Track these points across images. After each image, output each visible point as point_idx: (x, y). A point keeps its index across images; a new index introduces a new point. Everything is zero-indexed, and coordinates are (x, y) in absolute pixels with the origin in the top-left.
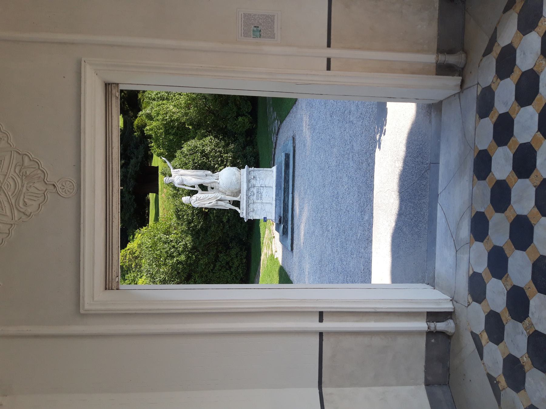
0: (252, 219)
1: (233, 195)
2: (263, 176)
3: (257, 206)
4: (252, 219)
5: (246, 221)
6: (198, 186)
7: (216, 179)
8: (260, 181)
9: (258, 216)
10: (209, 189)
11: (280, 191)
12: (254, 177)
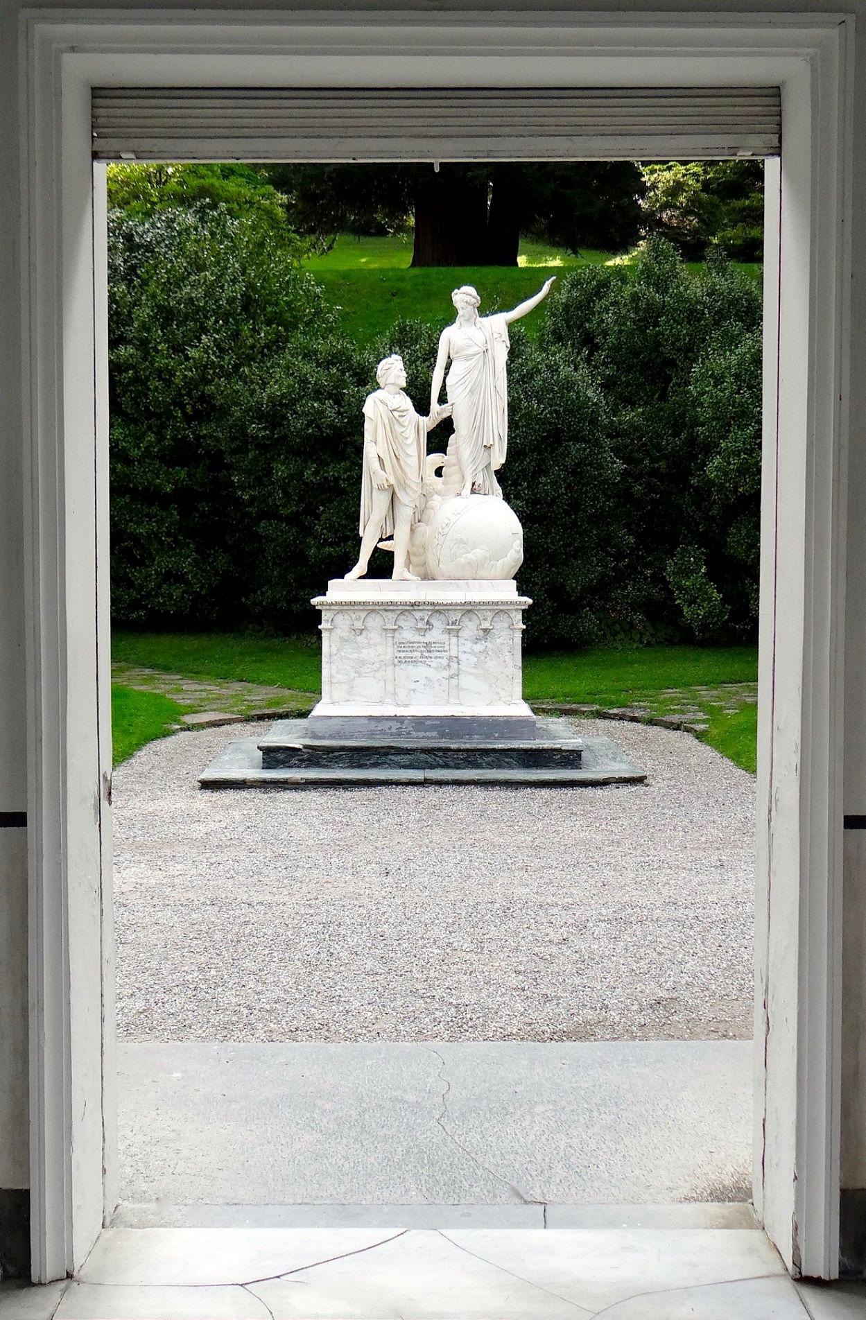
0: (319, 627)
3: (376, 646)
4: (319, 627)
5: (314, 601)
6: (445, 415)
7: (474, 484)
8: (473, 653)
9: (334, 650)
10: (436, 459)
12: (485, 630)
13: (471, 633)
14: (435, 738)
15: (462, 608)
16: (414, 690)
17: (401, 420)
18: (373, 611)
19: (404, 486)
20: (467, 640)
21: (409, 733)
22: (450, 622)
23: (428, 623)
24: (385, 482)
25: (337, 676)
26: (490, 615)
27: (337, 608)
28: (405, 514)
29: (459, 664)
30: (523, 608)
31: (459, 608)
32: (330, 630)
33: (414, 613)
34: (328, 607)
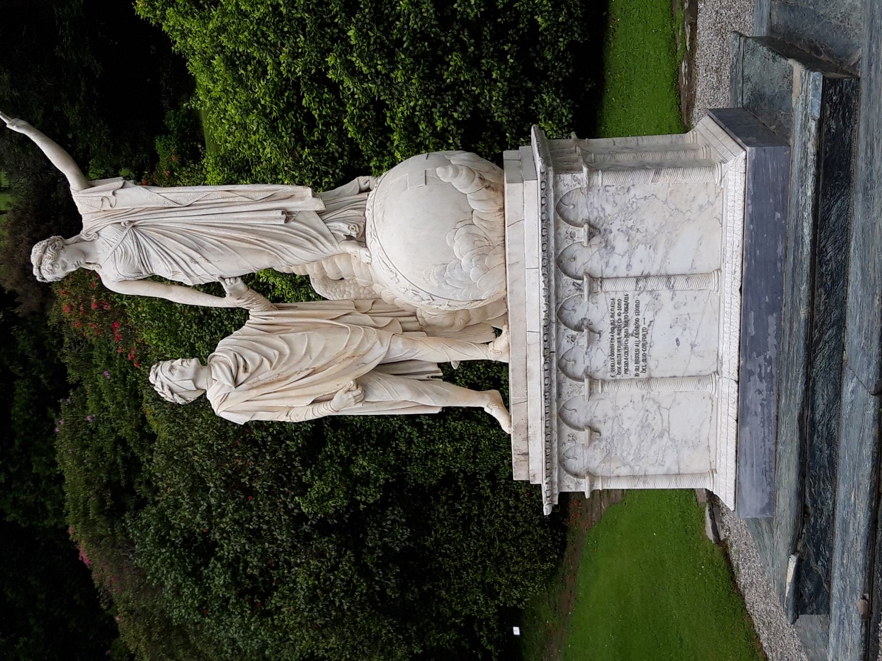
2: (650, 222)
8: (630, 252)
12: (593, 231)
13: (597, 256)
14: (779, 320)
15: (553, 278)
16: (693, 346)
17: (251, 368)
18: (560, 414)
19: (357, 357)
20: (607, 263)
21: (769, 362)
22: (578, 293)
23: (578, 328)
24: (350, 395)
25: (667, 464)
26: (565, 228)
27: (556, 474)
28: (400, 349)
31: (553, 283)
33: (562, 353)
34: (556, 486)
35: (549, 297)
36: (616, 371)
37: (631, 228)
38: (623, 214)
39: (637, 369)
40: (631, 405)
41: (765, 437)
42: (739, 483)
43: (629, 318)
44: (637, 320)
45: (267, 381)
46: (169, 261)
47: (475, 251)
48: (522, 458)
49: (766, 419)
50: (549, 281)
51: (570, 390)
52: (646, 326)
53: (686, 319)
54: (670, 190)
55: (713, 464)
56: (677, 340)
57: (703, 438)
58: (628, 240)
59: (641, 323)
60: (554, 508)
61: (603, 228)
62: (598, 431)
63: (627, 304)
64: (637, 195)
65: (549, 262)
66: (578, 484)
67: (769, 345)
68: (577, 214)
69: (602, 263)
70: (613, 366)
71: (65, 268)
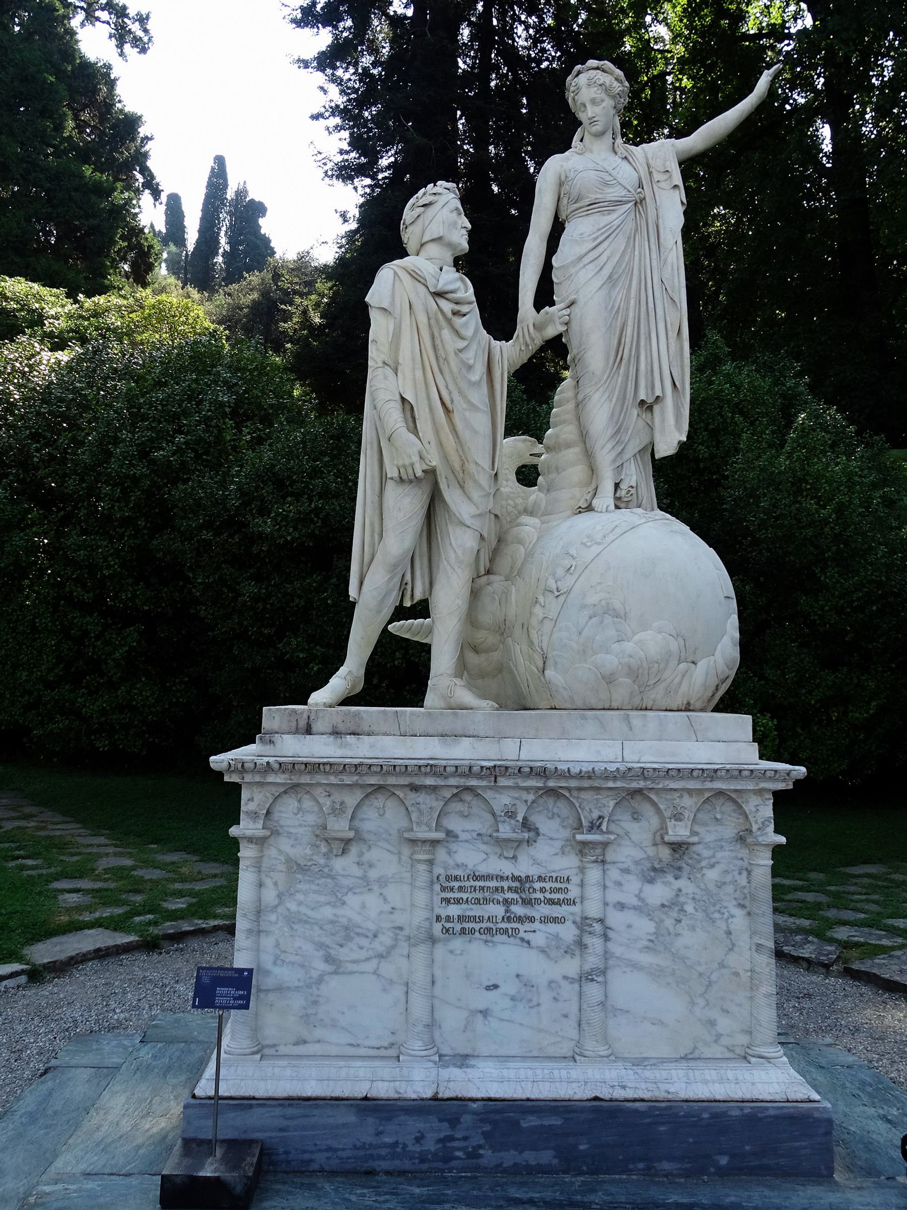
1: (481, 636)
4: (234, 831)
5: (218, 761)
7: (617, 486)
8: (642, 908)
9: (270, 895)
11: (546, 1157)
12: (678, 848)
13: (638, 854)
15: (619, 784)
16: (485, 1013)
18: (380, 788)
20: (626, 871)
21: (473, 1155)
24: (416, 458)
25: (277, 970)
27: (280, 778)
29: (606, 938)
30: (781, 786)
31: (611, 784)
32: (260, 842)
34: (258, 778)
35: (590, 778)
36: (447, 884)
37: (682, 910)
38: (705, 898)
39: (448, 919)
40: (387, 908)
41: (336, 1150)
42: (251, 1107)
43: (537, 907)
44: (531, 920)
45: (438, 342)
46: (597, 237)
47: (645, 664)
48: (302, 723)
49: (369, 1152)
50: (615, 779)
51: (422, 807)
52: (522, 934)
53: (530, 1001)
54: (741, 972)
55: (272, 1051)
56: (496, 987)
57: (319, 1033)
58: (663, 906)
59: (528, 926)
60: (220, 774)
61: (684, 865)
62: (344, 852)
63: (558, 903)
64: (734, 920)
65: (645, 779)
66: (254, 815)
67: (502, 1154)
68: (707, 825)
69: (629, 863)
70: (456, 878)
71: (594, 102)
